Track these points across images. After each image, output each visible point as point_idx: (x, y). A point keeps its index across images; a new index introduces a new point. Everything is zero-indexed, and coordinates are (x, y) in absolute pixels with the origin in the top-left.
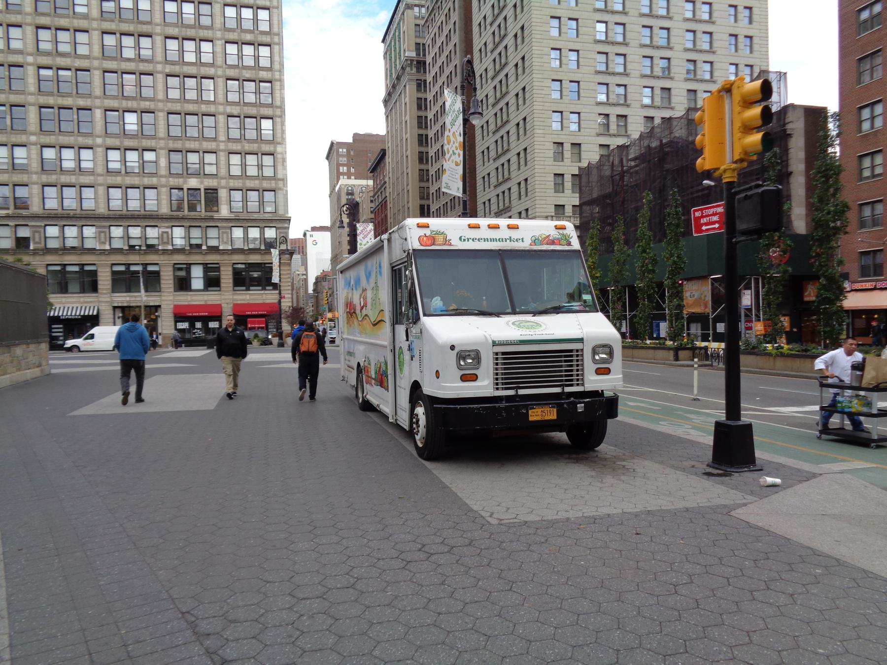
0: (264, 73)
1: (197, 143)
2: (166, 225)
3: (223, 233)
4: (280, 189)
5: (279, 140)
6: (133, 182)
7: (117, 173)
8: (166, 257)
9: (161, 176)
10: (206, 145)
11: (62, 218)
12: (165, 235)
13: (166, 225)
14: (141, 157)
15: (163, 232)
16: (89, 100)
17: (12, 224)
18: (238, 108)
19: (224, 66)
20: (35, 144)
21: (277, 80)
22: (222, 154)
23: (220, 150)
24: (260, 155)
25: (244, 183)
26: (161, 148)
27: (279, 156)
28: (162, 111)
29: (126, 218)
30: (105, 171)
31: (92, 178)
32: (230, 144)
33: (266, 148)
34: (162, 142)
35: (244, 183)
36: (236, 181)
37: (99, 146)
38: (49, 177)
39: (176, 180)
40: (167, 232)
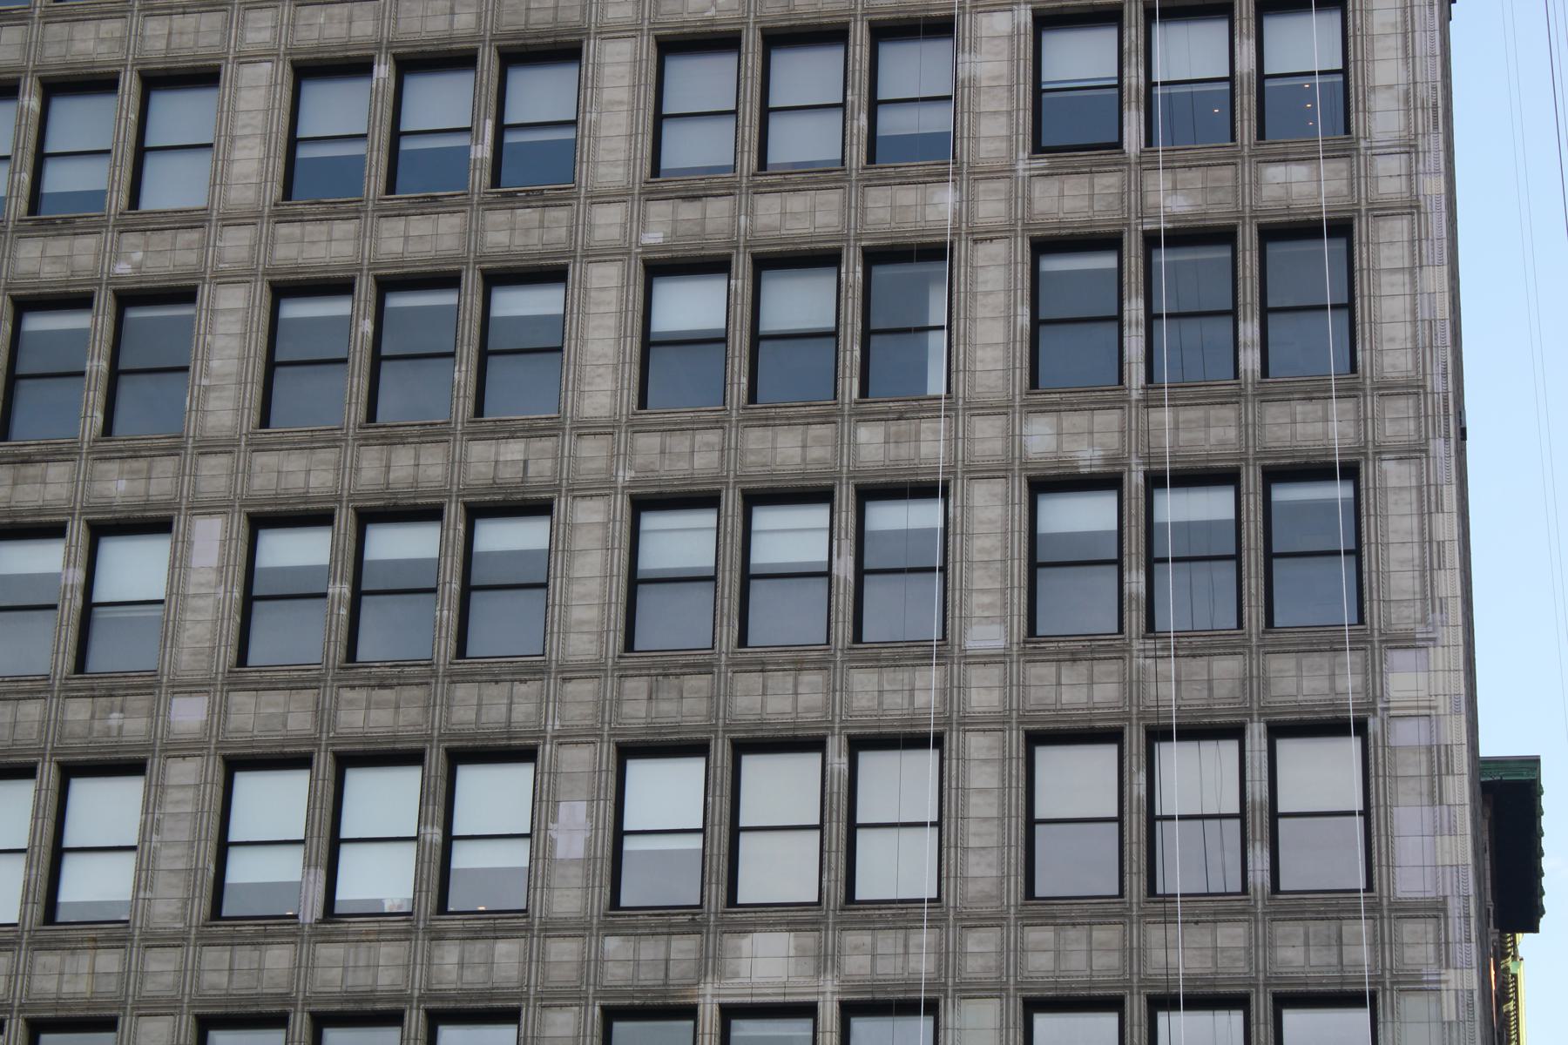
0: (1299, 172)
1: (812, 680)
4: (1413, 983)
5: (1404, 617)
6: (360, 981)
7: (274, 926)
9: (555, 928)
10: (873, 695)
16: (167, 465)
18: (1108, 420)
19: (1023, 163)
21: (1383, 211)
22: (979, 745)
23: (970, 723)
24: (1256, 734)
25: (1132, 953)
26: (566, 738)
27: (1406, 734)
28: (599, 489)
30: (203, 906)
31: (109, 961)
32: (1041, 673)
33: (1300, 682)
34: (582, 690)
35: (1132, 953)
37: (182, 749)
39: (651, 949)
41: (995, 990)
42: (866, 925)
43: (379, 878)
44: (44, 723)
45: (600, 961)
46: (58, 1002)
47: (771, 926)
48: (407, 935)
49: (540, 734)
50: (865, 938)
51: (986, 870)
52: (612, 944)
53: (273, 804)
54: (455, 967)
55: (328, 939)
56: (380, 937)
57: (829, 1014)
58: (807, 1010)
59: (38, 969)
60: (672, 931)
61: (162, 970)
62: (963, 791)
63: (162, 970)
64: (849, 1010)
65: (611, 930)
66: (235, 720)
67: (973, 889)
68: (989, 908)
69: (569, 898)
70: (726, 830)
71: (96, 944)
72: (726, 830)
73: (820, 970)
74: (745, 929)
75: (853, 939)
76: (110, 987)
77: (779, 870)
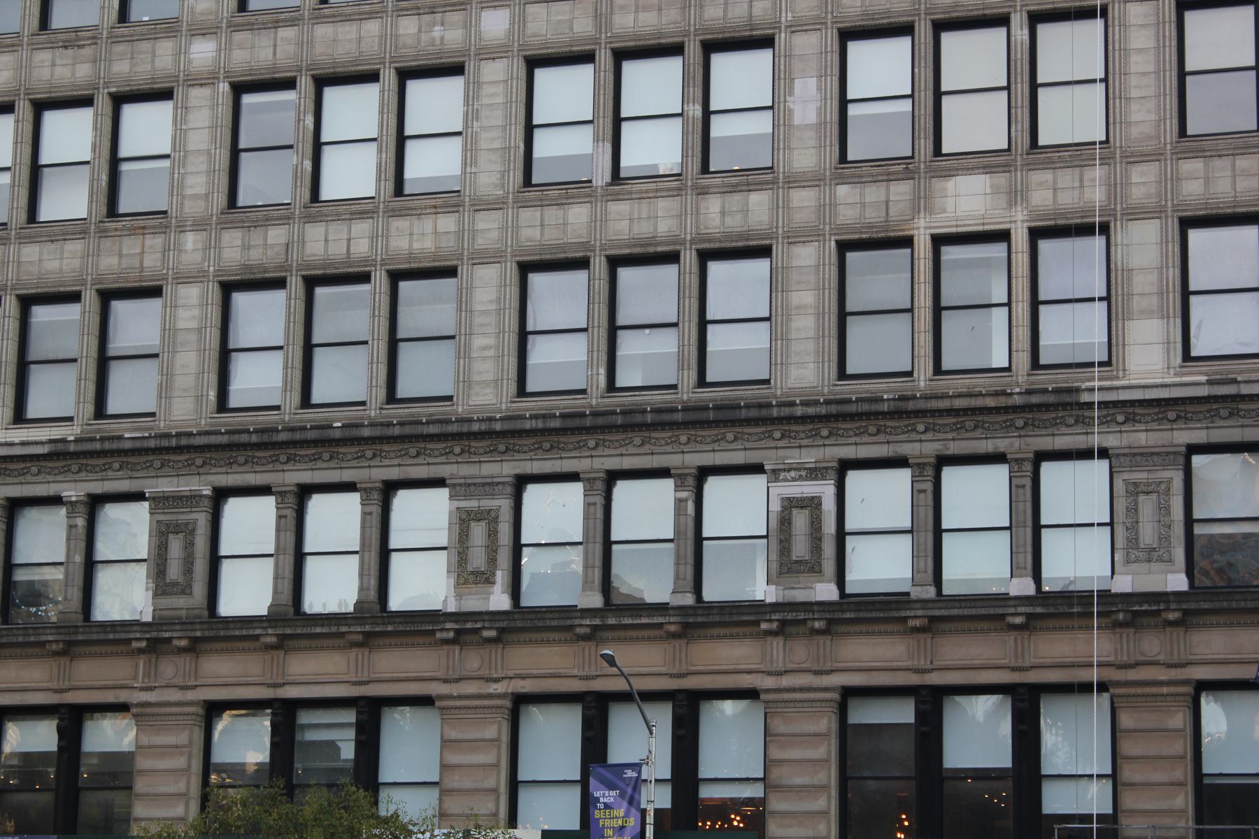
2: (809, 457)
3: (1135, 490)
6: (643, 229)
7: (574, 189)
8: (800, 651)
9: (794, 181)
11: (295, 452)
12: (800, 520)
13: (809, 457)
14: (701, 85)
15: (790, 504)
17: (72, 492)
20: (207, 80)
26: (796, 27)
29: (603, 433)
30: (517, 177)
31: (447, 223)
36: (1221, 166)
37: (491, 53)
38: (256, 237)
39: (874, 194)
40: (813, 504)
41: (1154, 213)
42: (1049, 165)
43: (654, 148)
44: (383, 37)
45: (833, 205)
46: (411, 257)
47: (970, 170)
48: (678, 192)
49: (776, 25)
50: (1048, 176)
51: (1146, 115)
52: (842, 191)
53: (566, 93)
54: (718, 215)
55: (617, 198)
56: (656, 195)
57: (1020, 238)
58: (1002, 236)
59: (393, 231)
60: (890, 178)
61: (488, 228)
62: (1125, 51)
63: (488, 228)
64: (1036, 234)
65: (840, 180)
66: (532, 28)
67: (1135, 132)
68: (1149, 146)
69: (806, 156)
70: (932, 94)
71: (436, 210)
72: (932, 94)
73: (1011, 204)
74: (948, 174)
75: (1037, 177)
76: (449, 243)
77: (975, 124)
